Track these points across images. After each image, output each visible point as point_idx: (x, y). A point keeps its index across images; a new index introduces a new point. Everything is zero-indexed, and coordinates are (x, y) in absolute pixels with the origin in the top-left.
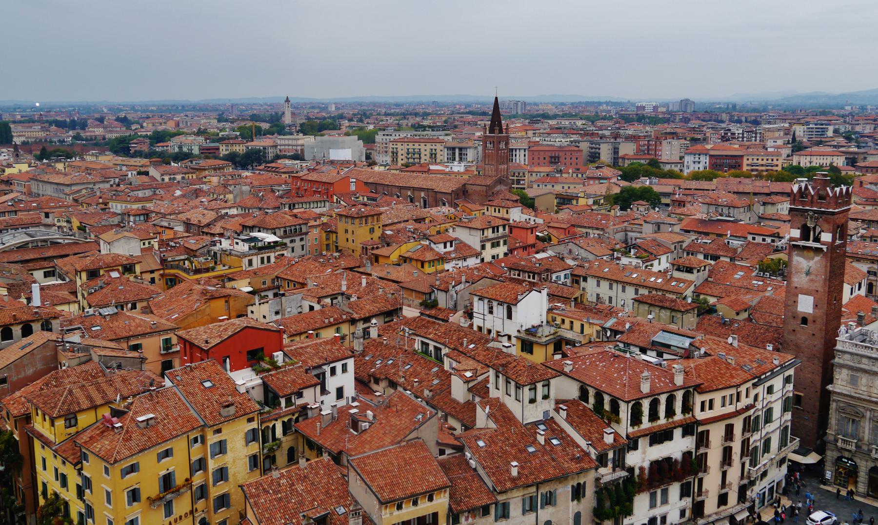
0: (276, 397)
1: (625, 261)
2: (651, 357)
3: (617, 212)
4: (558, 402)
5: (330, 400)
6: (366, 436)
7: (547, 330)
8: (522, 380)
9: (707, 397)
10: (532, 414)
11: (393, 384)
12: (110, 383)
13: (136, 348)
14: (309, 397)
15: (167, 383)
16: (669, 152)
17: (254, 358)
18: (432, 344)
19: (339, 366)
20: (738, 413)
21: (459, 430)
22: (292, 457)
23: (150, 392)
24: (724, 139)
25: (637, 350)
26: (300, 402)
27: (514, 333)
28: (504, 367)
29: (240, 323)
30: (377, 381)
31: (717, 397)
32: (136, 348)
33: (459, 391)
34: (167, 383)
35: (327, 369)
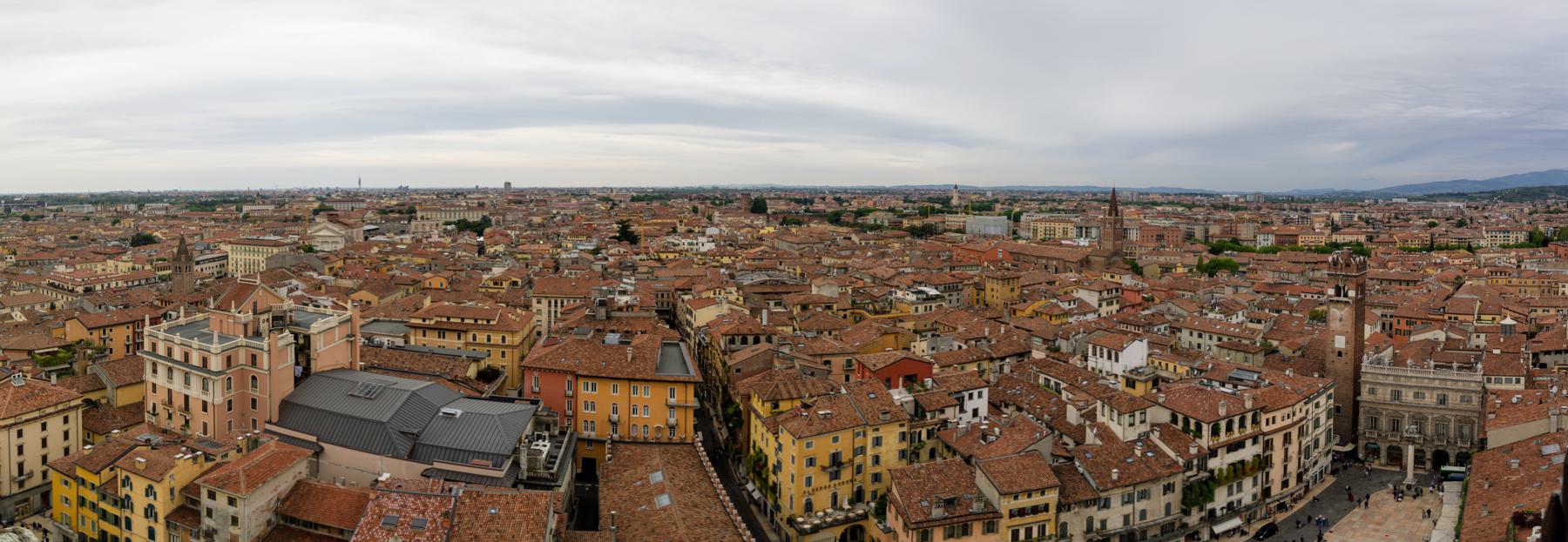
0: (924, 411)
1: (1211, 315)
2: (1228, 389)
3: (1204, 278)
4: (1153, 425)
5: (968, 417)
6: (992, 446)
7: (1148, 371)
8: (1123, 409)
9: (1270, 416)
10: (1132, 435)
11: (1020, 409)
12: (804, 384)
13: (827, 362)
14: (950, 413)
15: (843, 391)
16: (1245, 232)
17: (910, 381)
18: (1053, 381)
19: (975, 393)
20: (1294, 424)
21: (1072, 445)
22: (932, 454)
23: (832, 394)
24: (1285, 222)
25: (1216, 384)
26: (943, 417)
27: (1120, 373)
28: (1110, 398)
29: (901, 354)
30: (1007, 406)
31: (1278, 414)
32: (827, 362)
33: (1073, 416)
34: (843, 391)
35: (966, 394)
